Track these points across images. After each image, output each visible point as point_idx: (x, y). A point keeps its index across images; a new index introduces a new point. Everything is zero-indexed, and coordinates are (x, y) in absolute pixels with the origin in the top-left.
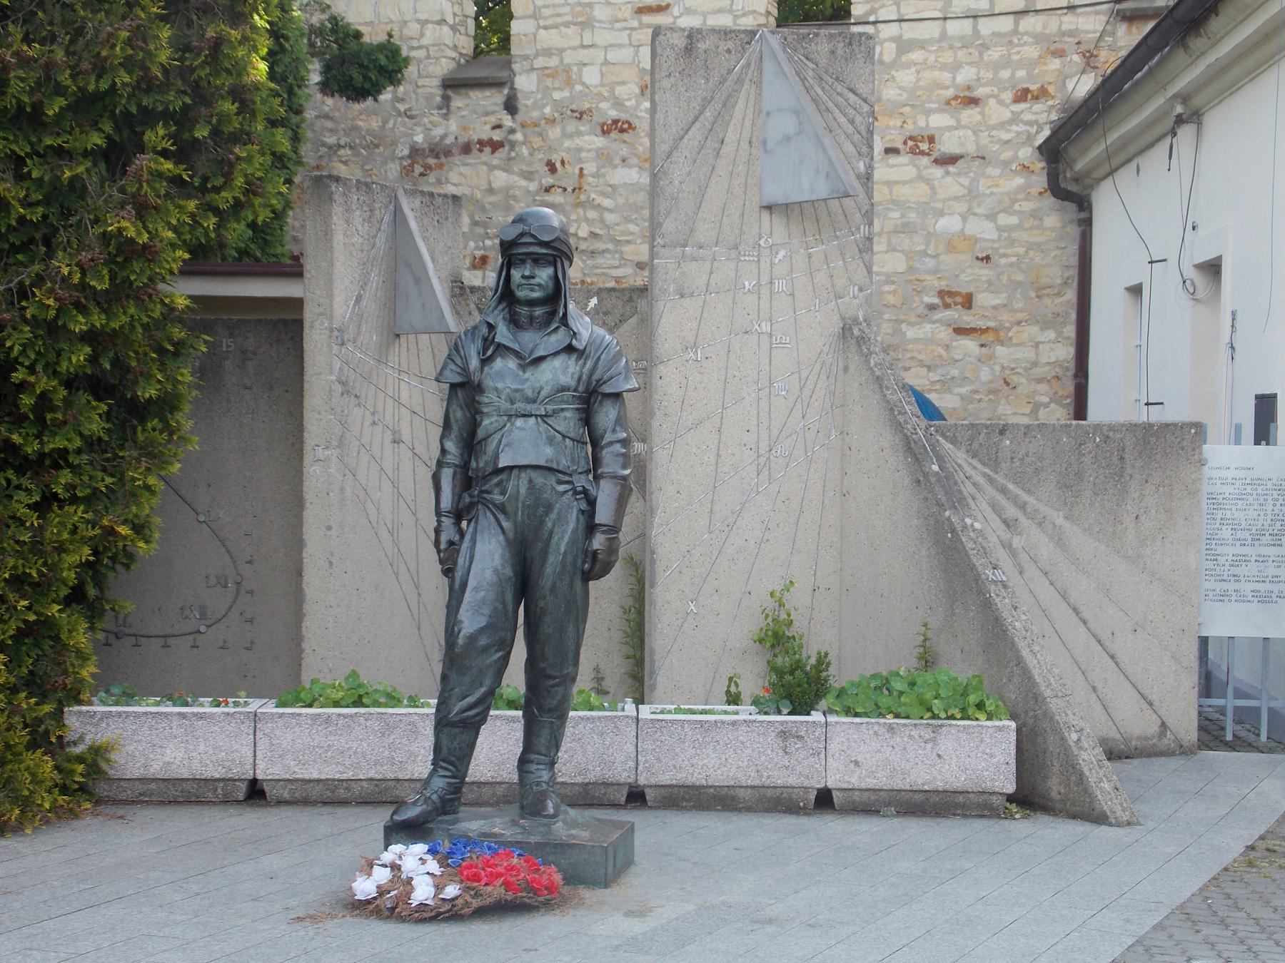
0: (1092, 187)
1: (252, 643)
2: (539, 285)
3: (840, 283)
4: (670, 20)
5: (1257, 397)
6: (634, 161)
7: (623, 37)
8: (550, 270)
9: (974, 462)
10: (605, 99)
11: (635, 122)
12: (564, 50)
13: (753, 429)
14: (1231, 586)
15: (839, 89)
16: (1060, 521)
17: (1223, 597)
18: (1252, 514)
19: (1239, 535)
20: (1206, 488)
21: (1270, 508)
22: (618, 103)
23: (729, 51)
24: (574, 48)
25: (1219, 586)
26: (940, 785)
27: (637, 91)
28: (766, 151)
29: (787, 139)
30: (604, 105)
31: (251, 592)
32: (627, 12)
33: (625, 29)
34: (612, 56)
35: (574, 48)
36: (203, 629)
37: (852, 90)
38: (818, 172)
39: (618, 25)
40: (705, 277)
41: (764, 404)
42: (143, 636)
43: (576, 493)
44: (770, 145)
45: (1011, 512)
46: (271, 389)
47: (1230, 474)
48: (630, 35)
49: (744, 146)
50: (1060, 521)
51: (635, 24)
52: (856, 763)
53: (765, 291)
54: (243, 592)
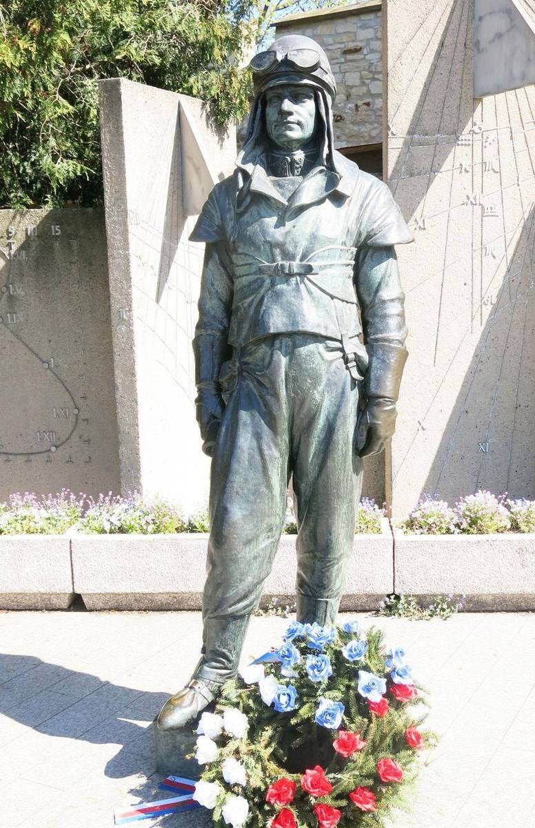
1: (90, 458)
2: (299, 123)
4: (362, 56)
6: (343, 138)
8: (310, 105)
11: (344, 116)
13: (469, 282)
27: (345, 98)
28: (478, 50)
29: (499, 36)
31: (87, 420)
32: (338, 54)
33: (338, 63)
36: (53, 449)
38: (529, 60)
40: (430, 159)
41: (477, 262)
42: (11, 454)
43: (346, 361)
44: (482, 45)
46: (90, 264)
48: (340, 67)
49: (461, 47)
51: (343, 60)
53: (478, 168)
54: (80, 421)
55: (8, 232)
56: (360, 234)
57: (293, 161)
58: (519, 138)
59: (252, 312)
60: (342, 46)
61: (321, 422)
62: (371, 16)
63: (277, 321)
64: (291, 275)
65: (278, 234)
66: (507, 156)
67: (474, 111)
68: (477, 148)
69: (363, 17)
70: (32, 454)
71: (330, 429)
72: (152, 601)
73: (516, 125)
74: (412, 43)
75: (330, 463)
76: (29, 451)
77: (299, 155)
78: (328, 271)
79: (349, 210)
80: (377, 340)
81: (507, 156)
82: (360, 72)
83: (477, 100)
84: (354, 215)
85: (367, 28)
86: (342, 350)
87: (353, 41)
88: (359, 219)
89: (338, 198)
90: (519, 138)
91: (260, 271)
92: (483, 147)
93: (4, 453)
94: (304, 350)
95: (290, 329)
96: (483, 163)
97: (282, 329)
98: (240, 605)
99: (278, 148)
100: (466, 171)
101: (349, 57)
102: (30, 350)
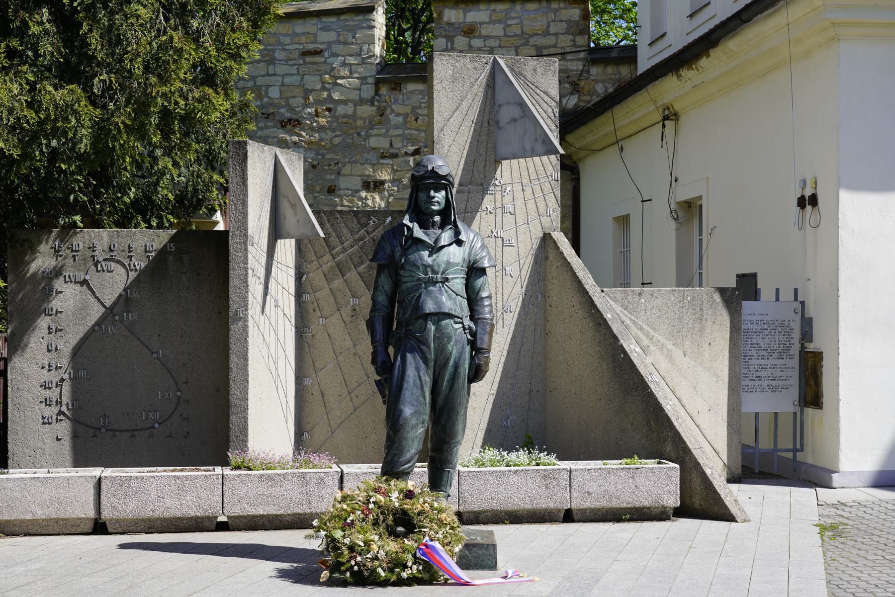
0: (580, 160)
2: (438, 202)
3: (542, 207)
4: (323, 59)
5: (737, 276)
7: (294, 70)
8: (443, 193)
9: (625, 312)
10: (282, 107)
12: (257, 77)
14: (757, 383)
15: (538, 92)
16: (670, 347)
17: (752, 389)
18: (767, 340)
19: (761, 353)
20: (743, 326)
21: (777, 337)
22: (291, 109)
23: (475, 68)
24: (263, 76)
25: (750, 383)
26: (638, 505)
29: (514, 120)
30: (282, 110)
32: (296, 55)
33: (295, 65)
34: (287, 80)
35: (263, 76)
37: (546, 93)
38: (536, 140)
39: (291, 63)
40: (464, 203)
41: (499, 280)
42: (118, 431)
43: (464, 329)
44: (501, 125)
45: (646, 342)
47: (755, 318)
48: (298, 69)
49: (485, 124)
50: (670, 347)
51: (301, 61)
52: (588, 493)
53: (499, 211)
55: (130, 247)
56: (470, 261)
57: (434, 222)
58: (528, 190)
59: (413, 302)
60: (301, 47)
61: (451, 362)
62: (333, 19)
63: (430, 306)
64: (437, 282)
65: (429, 261)
66: (519, 203)
67: (496, 170)
68: (498, 197)
69: (324, 19)
70: (137, 430)
71: (457, 366)
72: (281, 521)
73: (525, 181)
74: (451, 121)
75: (456, 385)
76: (135, 427)
77: (437, 218)
78: (455, 281)
79: (466, 247)
80: (480, 319)
81: (519, 203)
82: (321, 75)
83: (497, 162)
84: (467, 252)
85: (328, 30)
86: (462, 323)
87: (312, 43)
88: (470, 254)
89: (459, 243)
90: (528, 190)
91: (419, 279)
92: (503, 196)
93: (111, 430)
94: (444, 323)
95: (437, 311)
96: (503, 207)
97: (433, 311)
98: (407, 466)
99: (425, 214)
100: (491, 213)
101: (308, 59)
102: (142, 342)
